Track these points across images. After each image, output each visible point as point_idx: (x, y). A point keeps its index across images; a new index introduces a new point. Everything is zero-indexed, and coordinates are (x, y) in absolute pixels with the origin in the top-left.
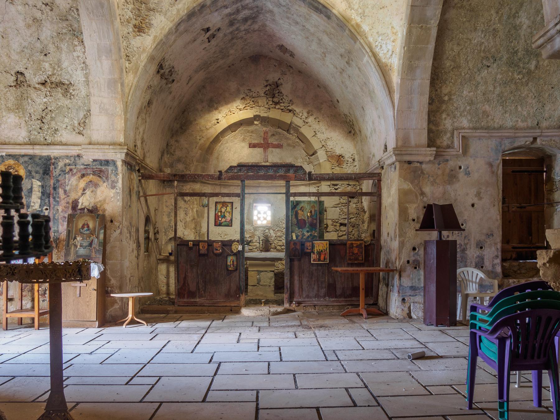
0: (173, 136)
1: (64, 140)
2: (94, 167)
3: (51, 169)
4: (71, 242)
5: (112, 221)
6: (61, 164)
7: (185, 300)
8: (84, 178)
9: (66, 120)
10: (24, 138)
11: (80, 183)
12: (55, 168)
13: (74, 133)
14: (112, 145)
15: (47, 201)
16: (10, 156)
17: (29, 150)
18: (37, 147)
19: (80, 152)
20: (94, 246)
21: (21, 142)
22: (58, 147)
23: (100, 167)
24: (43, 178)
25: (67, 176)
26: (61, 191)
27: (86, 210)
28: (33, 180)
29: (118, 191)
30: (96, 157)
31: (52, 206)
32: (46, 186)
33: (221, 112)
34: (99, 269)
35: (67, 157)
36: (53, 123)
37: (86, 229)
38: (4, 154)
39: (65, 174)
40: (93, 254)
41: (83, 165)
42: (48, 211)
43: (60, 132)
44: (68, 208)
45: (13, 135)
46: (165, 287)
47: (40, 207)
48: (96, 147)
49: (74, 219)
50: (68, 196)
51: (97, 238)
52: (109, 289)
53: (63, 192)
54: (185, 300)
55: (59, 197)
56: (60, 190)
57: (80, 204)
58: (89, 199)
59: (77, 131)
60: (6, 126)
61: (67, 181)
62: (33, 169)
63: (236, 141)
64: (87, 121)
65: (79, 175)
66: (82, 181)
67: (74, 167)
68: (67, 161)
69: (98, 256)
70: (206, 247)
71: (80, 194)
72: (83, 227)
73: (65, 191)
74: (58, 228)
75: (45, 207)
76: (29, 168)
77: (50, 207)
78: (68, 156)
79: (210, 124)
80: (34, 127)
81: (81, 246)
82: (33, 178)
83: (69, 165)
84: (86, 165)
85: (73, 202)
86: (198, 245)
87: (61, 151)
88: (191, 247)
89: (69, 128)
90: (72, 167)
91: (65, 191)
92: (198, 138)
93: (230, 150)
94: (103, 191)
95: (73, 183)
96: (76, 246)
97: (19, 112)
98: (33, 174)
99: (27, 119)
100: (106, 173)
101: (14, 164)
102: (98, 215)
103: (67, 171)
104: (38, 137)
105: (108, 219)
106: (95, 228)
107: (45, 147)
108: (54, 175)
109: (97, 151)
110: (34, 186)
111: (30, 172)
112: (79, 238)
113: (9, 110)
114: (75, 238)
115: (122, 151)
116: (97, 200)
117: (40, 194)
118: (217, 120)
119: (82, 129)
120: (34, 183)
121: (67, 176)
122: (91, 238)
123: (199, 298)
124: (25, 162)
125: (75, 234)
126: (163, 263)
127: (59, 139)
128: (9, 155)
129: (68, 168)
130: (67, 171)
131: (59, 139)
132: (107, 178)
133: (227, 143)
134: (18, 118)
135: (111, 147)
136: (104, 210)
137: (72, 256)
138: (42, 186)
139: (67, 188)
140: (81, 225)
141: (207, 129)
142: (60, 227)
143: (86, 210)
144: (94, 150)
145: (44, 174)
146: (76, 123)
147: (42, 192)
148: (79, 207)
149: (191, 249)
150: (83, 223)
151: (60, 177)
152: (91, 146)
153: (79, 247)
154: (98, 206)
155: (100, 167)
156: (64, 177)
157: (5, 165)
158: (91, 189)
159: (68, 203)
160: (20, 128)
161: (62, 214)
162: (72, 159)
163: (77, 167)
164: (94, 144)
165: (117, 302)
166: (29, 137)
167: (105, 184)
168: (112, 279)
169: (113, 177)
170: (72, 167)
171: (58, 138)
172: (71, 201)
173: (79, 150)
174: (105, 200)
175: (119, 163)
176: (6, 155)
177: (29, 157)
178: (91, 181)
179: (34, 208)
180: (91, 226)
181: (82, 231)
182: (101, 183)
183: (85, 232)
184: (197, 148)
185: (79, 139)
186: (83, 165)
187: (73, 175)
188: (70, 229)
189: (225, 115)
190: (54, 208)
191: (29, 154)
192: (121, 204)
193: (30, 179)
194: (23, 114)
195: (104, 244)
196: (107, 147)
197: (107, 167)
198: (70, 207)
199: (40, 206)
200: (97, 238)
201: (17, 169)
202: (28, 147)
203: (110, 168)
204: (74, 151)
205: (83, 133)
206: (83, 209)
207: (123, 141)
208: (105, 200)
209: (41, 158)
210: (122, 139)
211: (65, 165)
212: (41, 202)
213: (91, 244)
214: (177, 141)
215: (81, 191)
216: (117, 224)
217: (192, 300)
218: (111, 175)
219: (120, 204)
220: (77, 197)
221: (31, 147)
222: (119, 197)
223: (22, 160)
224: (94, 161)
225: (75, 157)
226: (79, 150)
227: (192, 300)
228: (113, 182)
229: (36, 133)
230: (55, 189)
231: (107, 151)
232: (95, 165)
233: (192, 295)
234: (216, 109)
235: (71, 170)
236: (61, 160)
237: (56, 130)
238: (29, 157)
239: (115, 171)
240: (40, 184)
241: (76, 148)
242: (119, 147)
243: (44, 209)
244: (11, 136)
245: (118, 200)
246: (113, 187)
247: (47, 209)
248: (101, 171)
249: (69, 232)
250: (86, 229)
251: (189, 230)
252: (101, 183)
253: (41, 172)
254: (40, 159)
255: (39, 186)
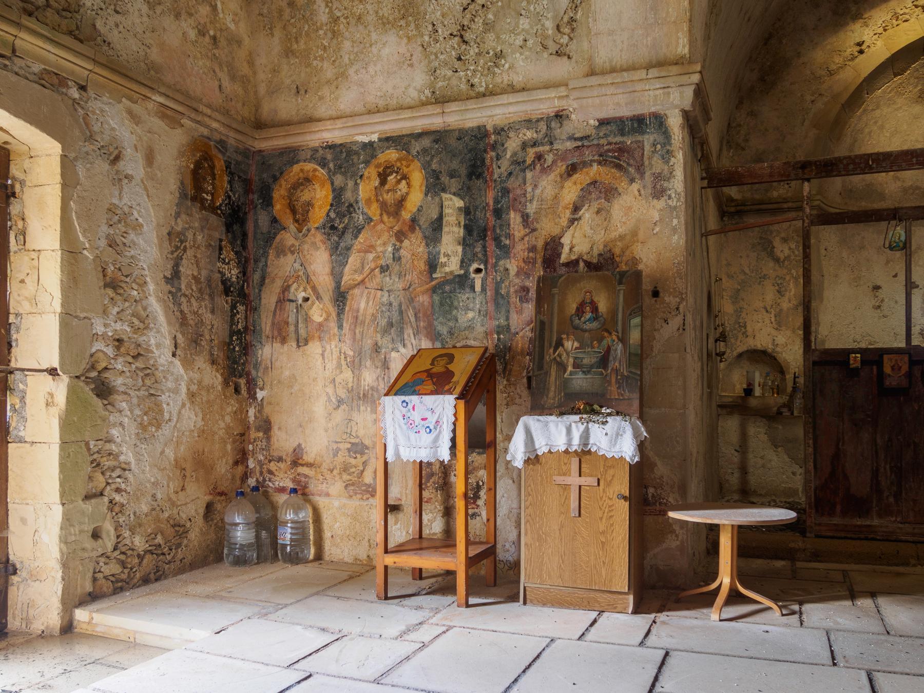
0: (741, 102)
1: (518, 79)
2: (602, 141)
3: (488, 162)
4: (550, 354)
5: (656, 294)
6: (512, 144)
7: (836, 520)
8: (575, 176)
9: (524, 23)
10: (420, 91)
11: (565, 191)
12: (498, 158)
13: (545, 55)
14: (654, 67)
15: (478, 249)
16: (389, 141)
17: (433, 120)
18: (453, 107)
19: (563, 104)
20: (613, 364)
21: (412, 103)
22: (505, 99)
23: (619, 139)
24: (469, 188)
25: (529, 175)
26: (514, 218)
27: (582, 264)
28: (444, 196)
29: (673, 203)
30: (604, 114)
31: (492, 261)
32: (476, 208)
33: (871, 23)
34: (636, 435)
35: (529, 123)
36: (491, 36)
37: (588, 315)
38: (375, 137)
39: (524, 170)
40: (614, 388)
41: (572, 138)
42: (482, 275)
43: (509, 59)
44: (534, 262)
45: (394, 87)
46: (737, 475)
47: (461, 267)
48: (609, 79)
49: (555, 291)
50: (534, 230)
51: (623, 340)
52: (651, 490)
53: (519, 219)
54: (836, 520)
55: (508, 236)
56: (512, 214)
57: (566, 249)
58: (589, 232)
59: (553, 48)
60: (379, 67)
61: (529, 189)
62: (444, 168)
63: (900, 101)
64: (579, 16)
65: (562, 167)
66: (568, 184)
67: (547, 148)
68: (529, 135)
69: (627, 394)
70: (905, 368)
71: (564, 222)
72: (580, 311)
73: (525, 218)
74: (507, 319)
75: (475, 266)
76: (434, 166)
77: (486, 265)
78: (529, 121)
79: (838, 60)
80: (442, 57)
81: (576, 366)
82: (444, 190)
83: (534, 145)
84: (581, 139)
85: (547, 244)
86: (880, 364)
87: (512, 109)
88: (857, 369)
89: (530, 43)
90: (541, 149)
91: (525, 218)
92: (809, 98)
93: (882, 127)
94: (630, 208)
95: (548, 192)
96: (562, 367)
97: (408, 25)
98: (445, 179)
99: (426, 38)
100: (637, 154)
101: (399, 160)
102: (622, 274)
103: (529, 161)
104: (454, 82)
105: (647, 286)
106: (613, 313)
107: (471, 105)
108: (496, 176)
109: (612, 90)
110: (447, 211)
111: (436, 175)
112: (568, 344)
113: (385, 23)
114: (559, 343)
115: (685, 79)
116: (614, 235)
117: (461, 232)
118: (860, 44)
119: (565, 40)
120: (446, 203)
121: (529, 175)
122: (605, 343)
123: (880, 516)
124: (425, 151)
125: (560, 333)
126: (730, 413)
127: (506, 78)
128: (387, 139)
129: (532, 152)
130: (529, 161)
131: (506, 78)
132: (640, 169)
133: (878, 107)
134: (405, 40)
135: (654, 73)
136: (635, 261)
137: (551, 394)
138: (467, 211)
139: (531, 209)
140: (574, 306)
141: (831, 73)
142: (514, 317)
143: (582, 264)
144: (604, 90)
145: (470, 176)
146: (549, 25)
147: (466, 226)
148: (564, 258)
149: (855, 372)
150: (579, 299)
151: (512, 179)
152: (594, 80)
153: (570, 368)
154: (617, 251)
155: (619, 139)
156: (520, 179)
157: (378, 166)
158: (595, 206)
159: (533, 249)
160: (411, 65)
161: (517, 281)
162: (543, 126)
163: (556, 146)
164: (603, 73)
165: (673, 532)
166: (432, 86)
167: (635, 186)
168: (659, 463)
169: (657, 165)
170: (540, 149)
171: (503, 77)
172: (540, 244)
173: (560, 98)
174: (634, 233)
175: (675, 122)
176: (380, 140)
177: (432, 137)
178: (594, 183)
179: (447, 269)
180: (603, 307)
181: (577, 321)
182: (623, 185)
183: (588, 326)
184: (807, 123)
185: (561, 69)
186: (572, 138)
187: (545, 170)
188: (545, 319)
189: (881, 30)
190: (495, 265)
191: (433, 128)
192: (682, 242)
193: (436, 194)
194: (417, 27)
195: (638, 358)
196: (642, 74)
197: (640, 138)
198: (539, 261)
199: (464, 263)
200: (623, 340)
201: (405, 170)
202: (431, 109)
203: (648, 140)
204: (544, 104)
205: (567, 50)
206: (576, 263)
207: (686, 50)
208: (634, 233)
209: (462, 134)
210: (682, 47)
211: (524, 146)
212: (464, 252)
213: (604, 361)
214: (752, 114)
215: (568, 214)
216: (670, 299)
217: (859, 522)
218: (650, 158)
219: (678, 240)
220: (556, 231)
221: (437, 109)
222: (675, 222)
223: (416, 147)
224: (603, 122)
225: (548, 120)
226: (560, 98)
227: (859, 522)
228: (658, 177)
229: (450, 73)
230: (498, 213)
231: (639, 87)
232: (606, 136)
233: (857, 506)
234: (857, 16)
235: (539, 157)
236: (512, 134)
237: (499, 55)
238: (432, 137)
239: (664, 145)
240: (460, 203)
241: (552, 93)
242: (675, 69)
243: (472, 269)
244: (391, 91)
245: (674, 230)
246: (658, 193)
247: (478, 271)
248: (622, 150)
249: (541, 328)
250: (588, 315)
251: (789, 333)
252: (623, 185)
253: (463, 171)
254: (459, 139)
255: (460, 209)
